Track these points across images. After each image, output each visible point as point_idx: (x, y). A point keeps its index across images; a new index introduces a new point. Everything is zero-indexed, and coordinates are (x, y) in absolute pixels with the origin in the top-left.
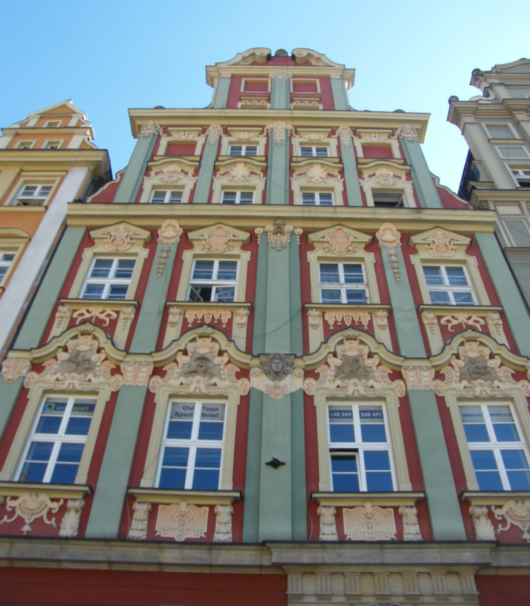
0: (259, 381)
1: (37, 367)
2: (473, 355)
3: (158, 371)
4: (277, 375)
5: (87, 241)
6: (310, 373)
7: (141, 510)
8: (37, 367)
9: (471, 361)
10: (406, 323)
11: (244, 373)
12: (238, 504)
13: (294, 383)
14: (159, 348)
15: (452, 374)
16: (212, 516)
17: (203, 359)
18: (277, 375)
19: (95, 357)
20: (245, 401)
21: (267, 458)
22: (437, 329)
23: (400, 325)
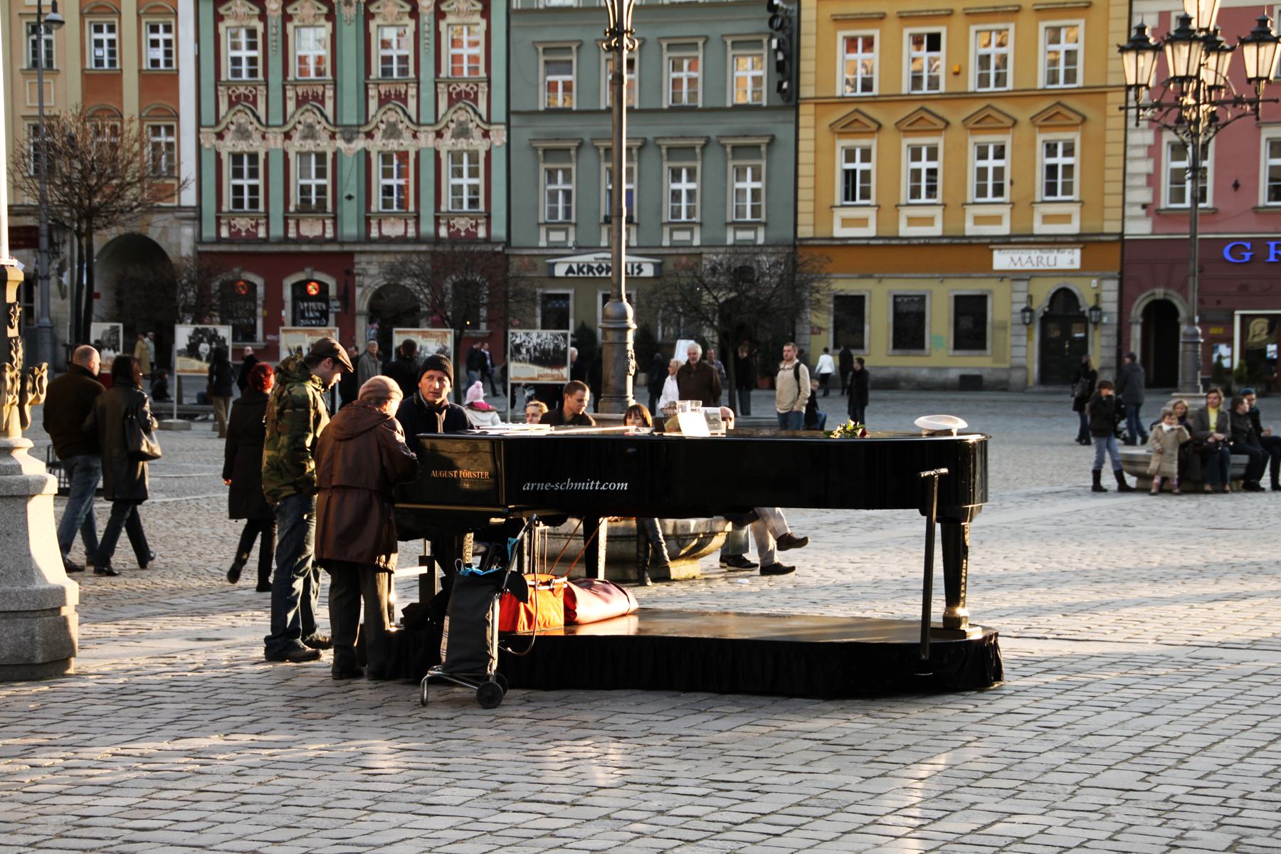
0: (340, 143)
1: (220, 136)
2: (462, 119)
3: (287, 136)
4: (349, 141)
5: (218, 18)
6: (369, 135)
7: (292, 223)
8: (220, 136)
9: (460, 124)
10: (427, 94)
11: (333, 136)
12: (335, 219)
13: (360, 143)
14: (285, 122)
15: (448, 134)
16: (324, 225)
17: (310, 127)
18: (349, 141)
19: (250, 128)
20: (335, 154)
21: (346, 194)
22: (446, 96)
23: (423, 94)
